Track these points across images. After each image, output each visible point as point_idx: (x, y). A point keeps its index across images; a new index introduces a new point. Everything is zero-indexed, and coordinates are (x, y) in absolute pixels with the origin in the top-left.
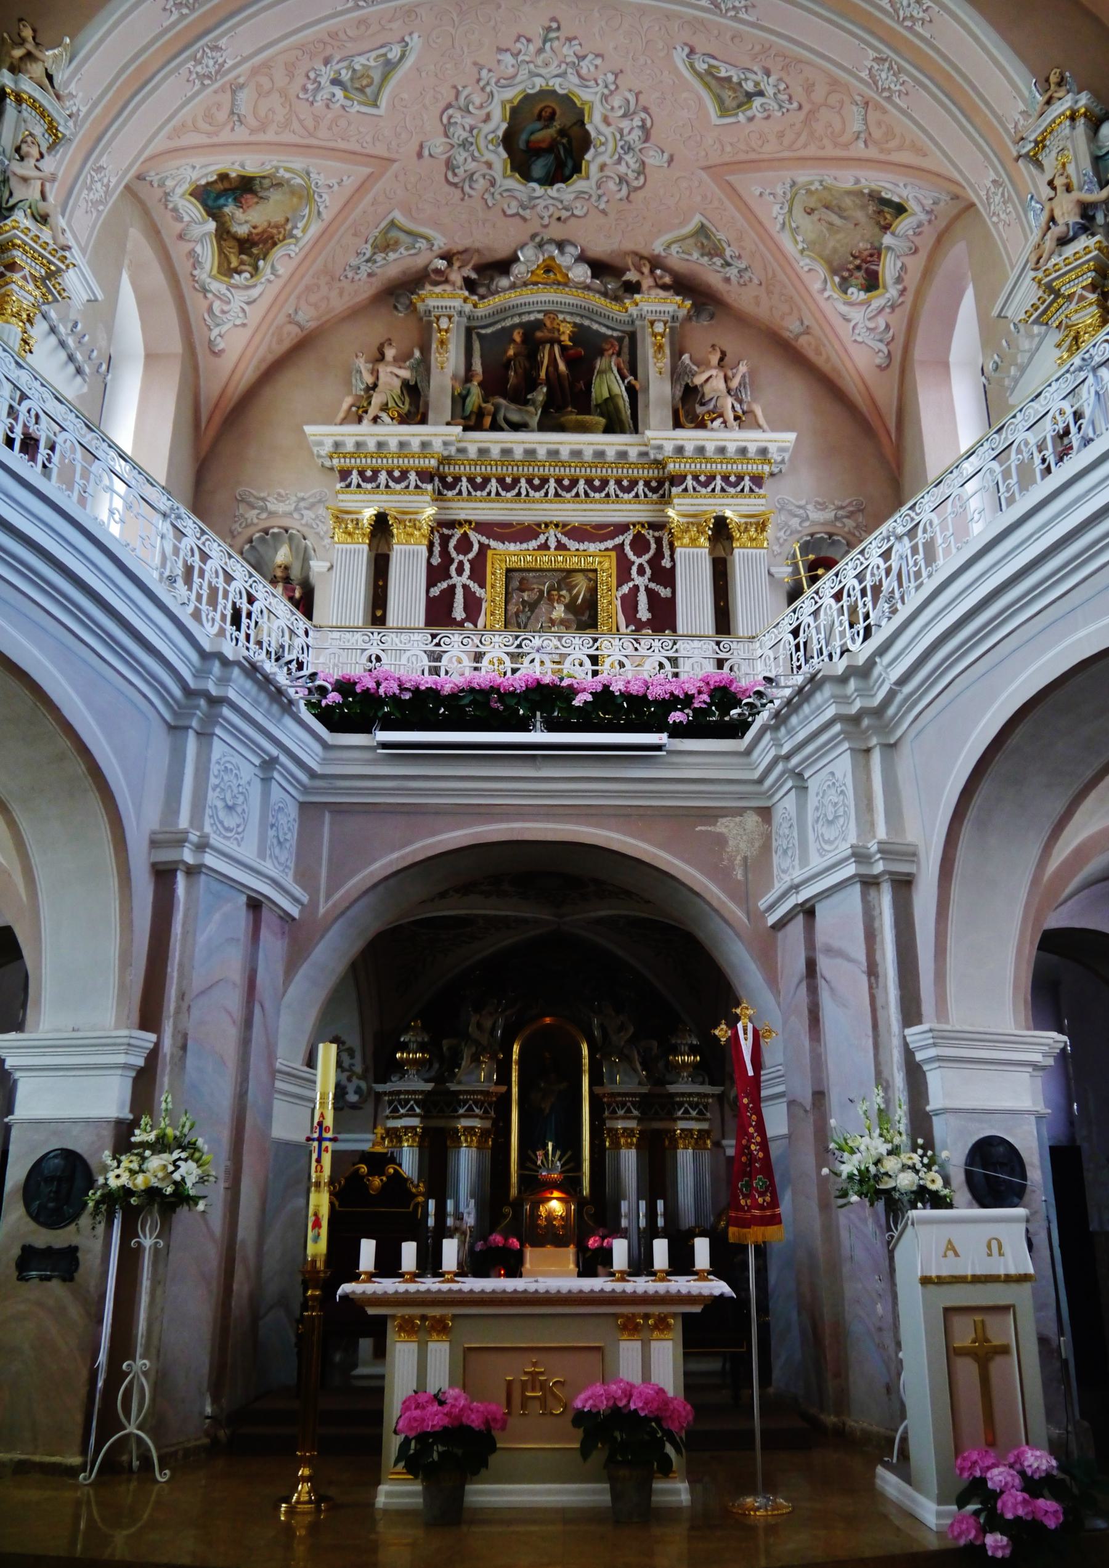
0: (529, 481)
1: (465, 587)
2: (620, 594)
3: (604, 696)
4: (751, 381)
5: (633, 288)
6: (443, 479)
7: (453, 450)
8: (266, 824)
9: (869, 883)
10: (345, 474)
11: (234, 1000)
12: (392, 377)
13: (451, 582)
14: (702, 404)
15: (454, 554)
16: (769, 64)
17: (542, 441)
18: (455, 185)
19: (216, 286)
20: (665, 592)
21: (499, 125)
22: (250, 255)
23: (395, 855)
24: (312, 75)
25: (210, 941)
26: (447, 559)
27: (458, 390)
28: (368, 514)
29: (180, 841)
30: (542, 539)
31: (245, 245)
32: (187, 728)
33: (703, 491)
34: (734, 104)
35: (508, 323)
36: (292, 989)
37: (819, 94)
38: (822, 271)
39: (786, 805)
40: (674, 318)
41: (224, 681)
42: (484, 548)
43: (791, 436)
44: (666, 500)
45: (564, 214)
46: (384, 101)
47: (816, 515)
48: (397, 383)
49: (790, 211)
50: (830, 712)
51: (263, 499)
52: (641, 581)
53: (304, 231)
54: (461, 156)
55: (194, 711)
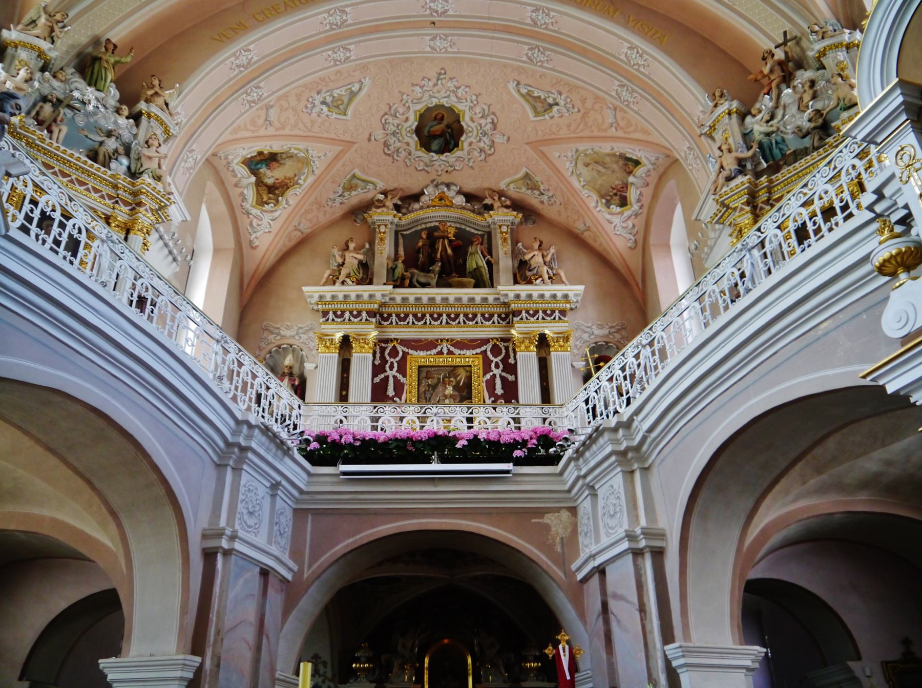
0: (431, 316)
1: (394, 377)
2: (485, 379)
3: (474, 441)
4: (557, 257)
5: (489, 208)
6: (381, 315)
7: (387, 298)
8: (273, 523)
9: (637, 553)
10: (325, 314)
11: (249, 634)
12: (353, 259)
13: (386, 374)
14: (530, 271)
15: (388, 358)
16: (561, 89)
17: (439, 293)
18: (389, 155)
19: (254, 211)
20: (511, 378)
21: (413, 123)
22: (274, 194)
23: (351, 540)
24: (310, 100)
25: (237, 597)
26: (384, 360)
27: (390, 266)
28: (338, 336)
29: (220, 535)
30: (439, 348)
31: (271, 189)
32: (227, 465)
33: (532, 319)
34: (542, 110)
35: (419, 228)
36: (286, 626)
37: (589, 104)
38: (595, 197)
39: (585, 506)
40: (513, 224)
41: (249, 437)
42: (405, 354)
43: (581, 288)
44: (510, 325)
45: (450, 169)
46: (350, 112)
47: (597, 332)
48: (356, 262)
49: (576, 165)
50: (609, 449)
51: (278, 328)
52: (497, 372)
53: (305, 181)
54: (392, 140)
55: (231, 455)
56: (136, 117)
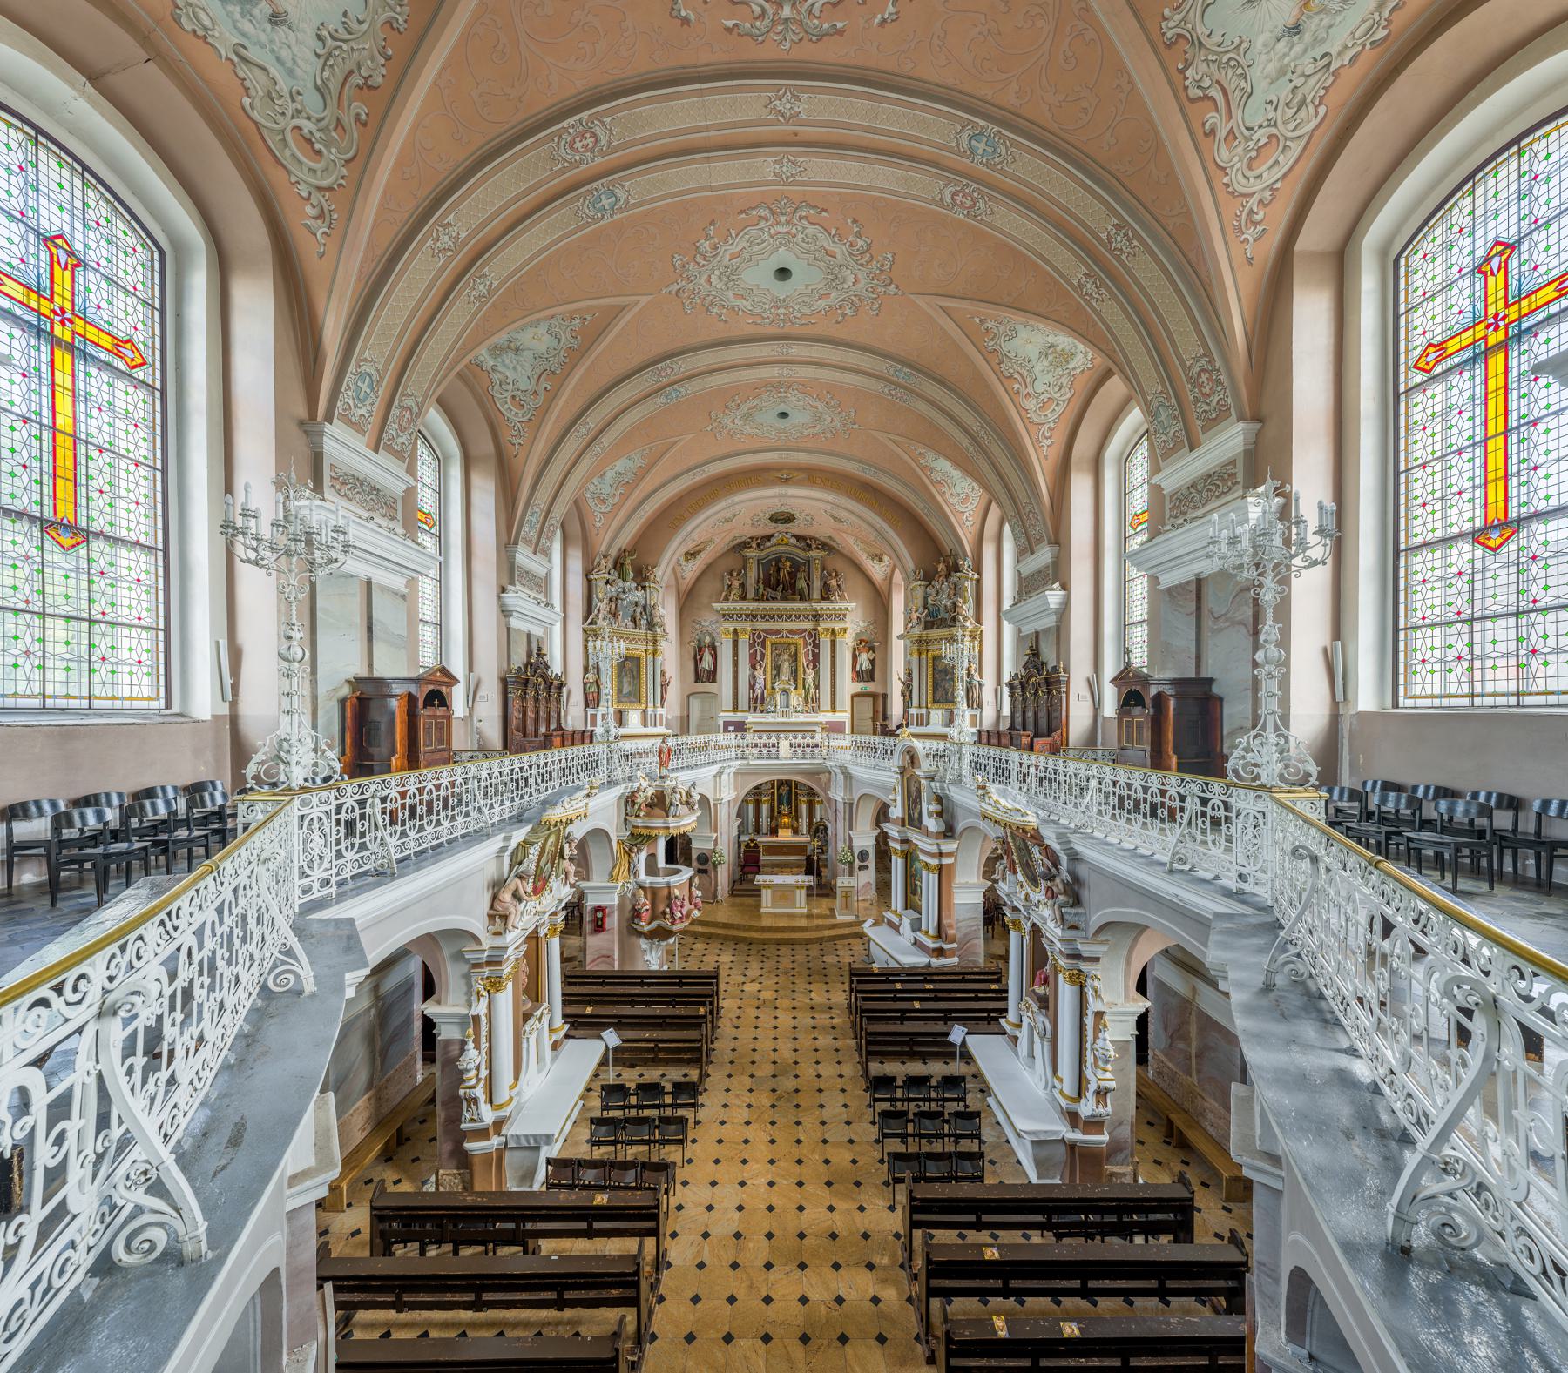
12: (736, 583)
17: (782, 605)
56: (644, 588)
